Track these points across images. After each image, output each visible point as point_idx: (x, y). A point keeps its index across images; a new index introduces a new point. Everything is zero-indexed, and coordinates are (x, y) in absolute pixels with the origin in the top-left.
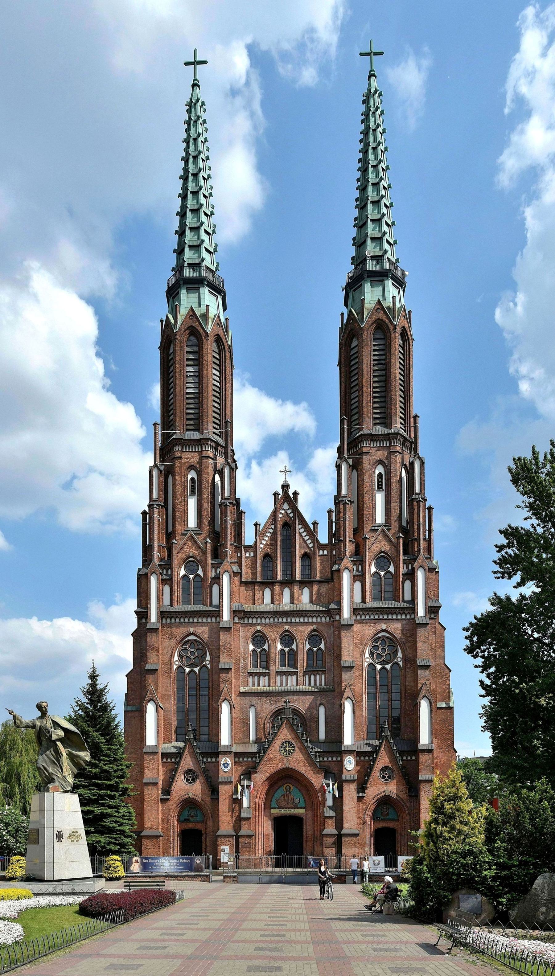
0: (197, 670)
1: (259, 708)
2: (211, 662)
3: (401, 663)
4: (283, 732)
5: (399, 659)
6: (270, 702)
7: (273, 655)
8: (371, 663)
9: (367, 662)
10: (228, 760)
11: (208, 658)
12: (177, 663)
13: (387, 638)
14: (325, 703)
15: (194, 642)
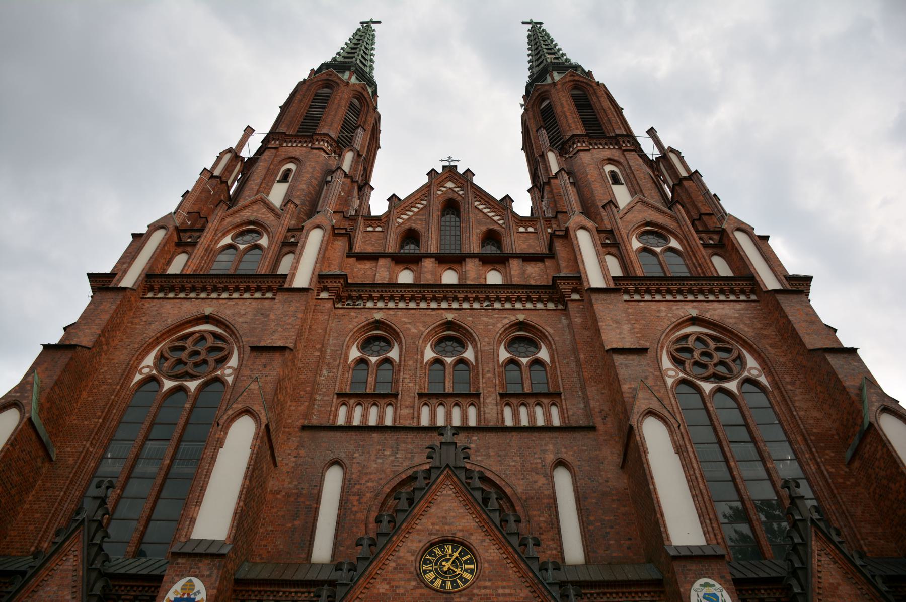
0: (192, 385)
1: (355, 469)
2: (238, 371)
3: (763, 380)
4: (433, 510)
5: (755, 373)
6: (394, 454)
7: (411, 363)
8: (683, 381)
9: (670, 377)
10: (199, 585)
11: (233, 362)
12: (146, 371)
13: (707, 335)
14: (568, 456)
15: (206, 335)
